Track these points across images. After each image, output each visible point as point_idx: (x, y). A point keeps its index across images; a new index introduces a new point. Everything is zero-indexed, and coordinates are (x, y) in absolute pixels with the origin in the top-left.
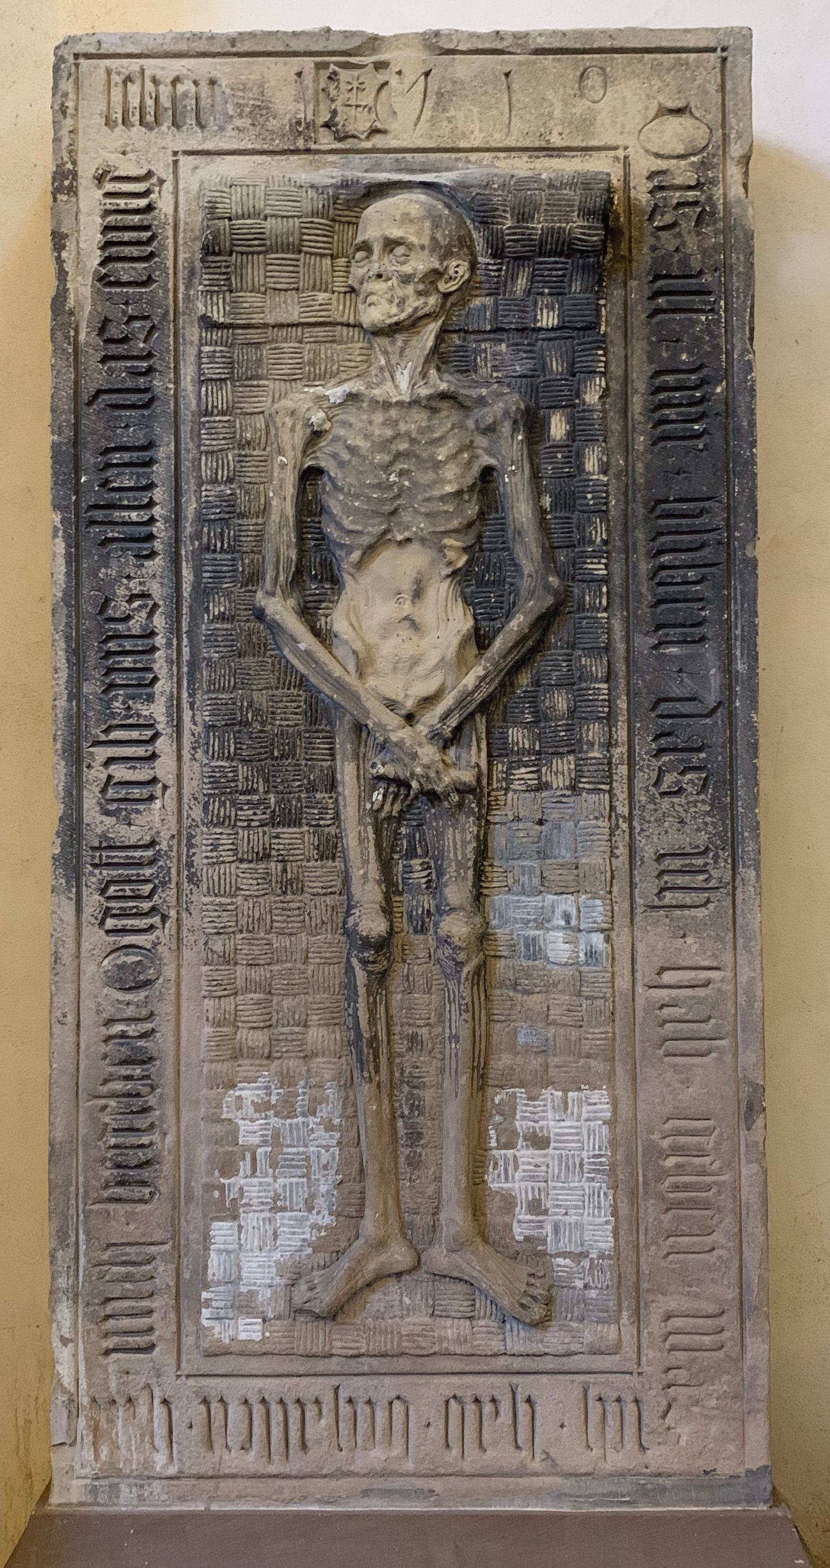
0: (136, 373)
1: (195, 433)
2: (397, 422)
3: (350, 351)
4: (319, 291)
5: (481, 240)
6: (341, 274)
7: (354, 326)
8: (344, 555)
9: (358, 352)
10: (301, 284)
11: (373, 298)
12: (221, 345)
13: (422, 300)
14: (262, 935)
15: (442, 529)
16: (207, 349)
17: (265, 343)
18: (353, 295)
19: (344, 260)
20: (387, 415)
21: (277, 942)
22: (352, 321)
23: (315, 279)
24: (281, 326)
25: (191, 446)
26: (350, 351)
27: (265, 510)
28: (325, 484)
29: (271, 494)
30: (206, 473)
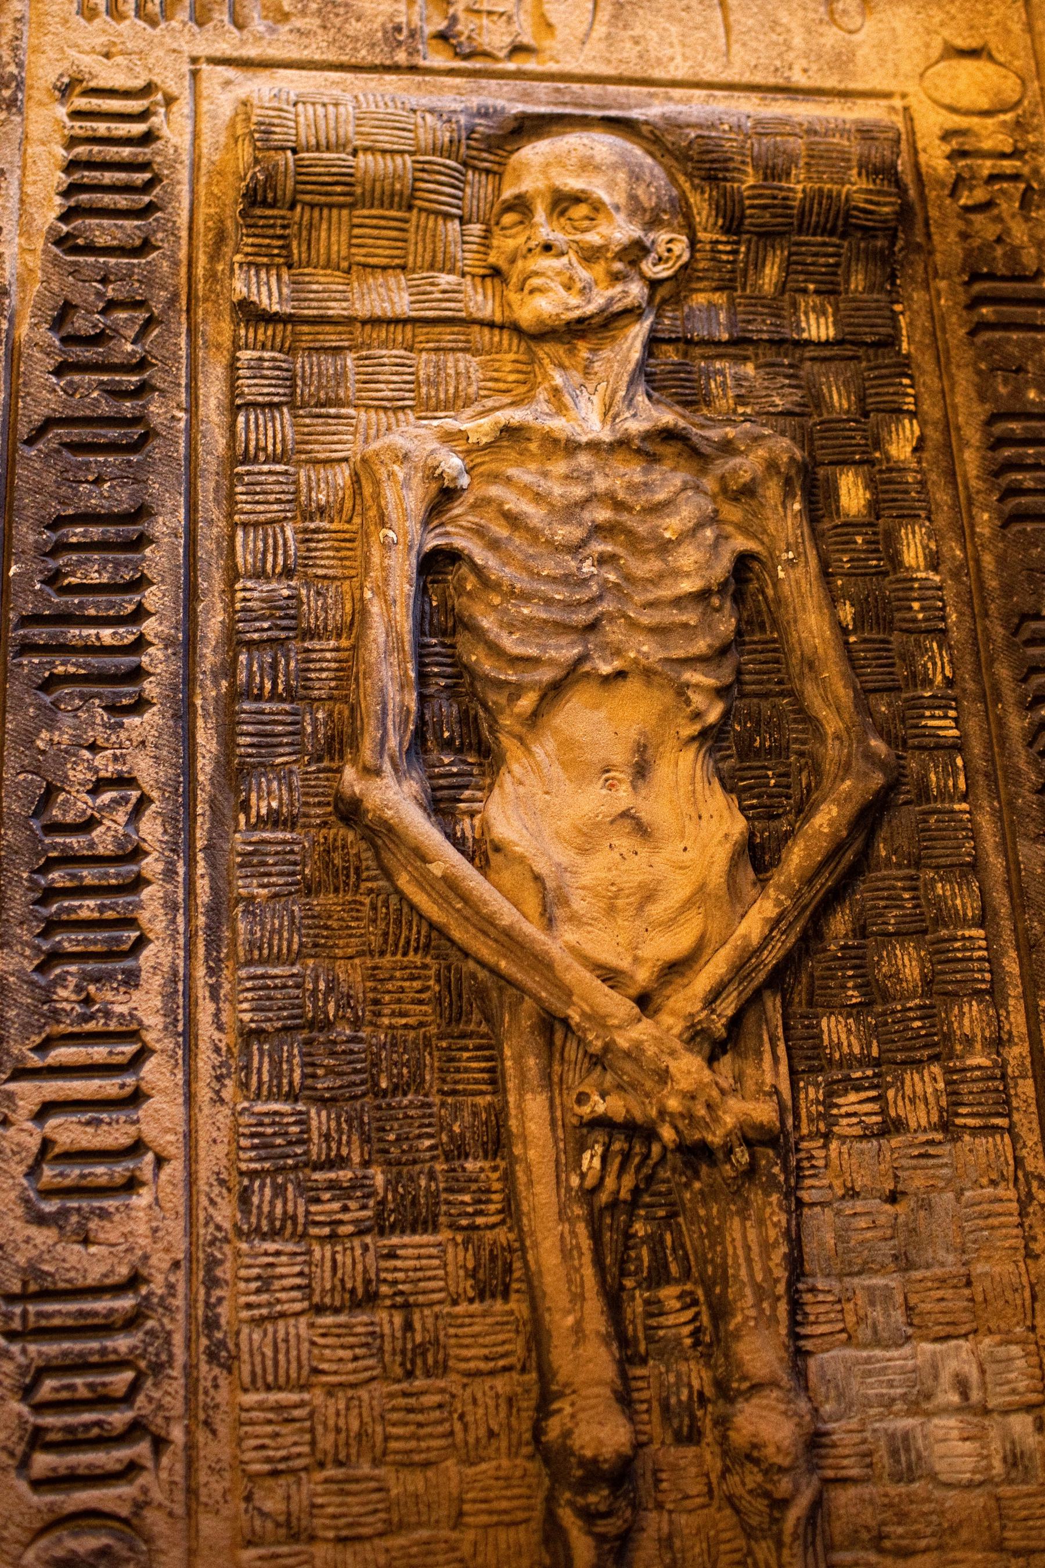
0: (117, 393)
1: (224, 492)
2: (589, 476)
3: (497, 365)
4: (442, 270)
5: (705, 205)
6: (474, 247)
7: (502, 327)
8: (503, 700)
9: (509, 367)
10: (411, 258)
11: (535, 282)
12: (273, 349)
13: (619, 288)
14: (366, 1469)
15: (681, 654)
16: (245, 355)
17: (349, 348)
18: (497, 281)
19: (479, 226)
20: (573, 463)
21: (403, 1485)
22: (498, 318)
23: (434, 251)
24: (375, 321)
25: (216, 514)
26: (497, 365)
27: (357, 621)
28: (462, 580)
29: (368, 595)
30: (243, 559)
